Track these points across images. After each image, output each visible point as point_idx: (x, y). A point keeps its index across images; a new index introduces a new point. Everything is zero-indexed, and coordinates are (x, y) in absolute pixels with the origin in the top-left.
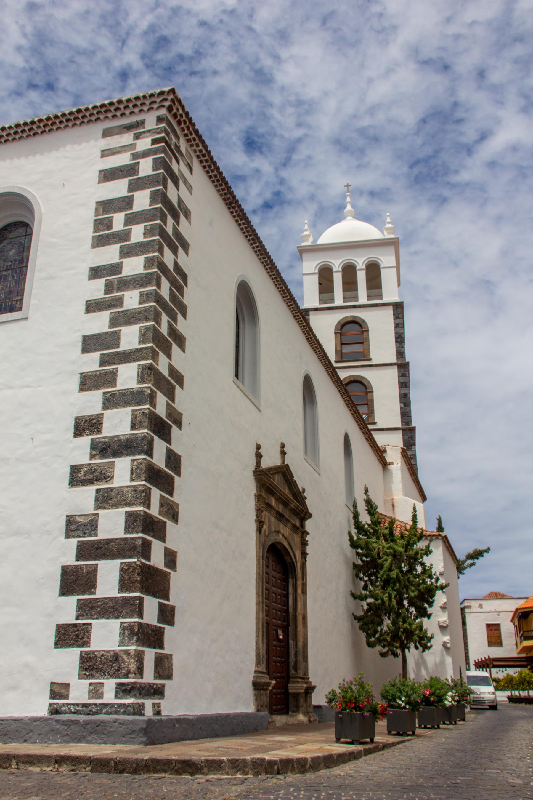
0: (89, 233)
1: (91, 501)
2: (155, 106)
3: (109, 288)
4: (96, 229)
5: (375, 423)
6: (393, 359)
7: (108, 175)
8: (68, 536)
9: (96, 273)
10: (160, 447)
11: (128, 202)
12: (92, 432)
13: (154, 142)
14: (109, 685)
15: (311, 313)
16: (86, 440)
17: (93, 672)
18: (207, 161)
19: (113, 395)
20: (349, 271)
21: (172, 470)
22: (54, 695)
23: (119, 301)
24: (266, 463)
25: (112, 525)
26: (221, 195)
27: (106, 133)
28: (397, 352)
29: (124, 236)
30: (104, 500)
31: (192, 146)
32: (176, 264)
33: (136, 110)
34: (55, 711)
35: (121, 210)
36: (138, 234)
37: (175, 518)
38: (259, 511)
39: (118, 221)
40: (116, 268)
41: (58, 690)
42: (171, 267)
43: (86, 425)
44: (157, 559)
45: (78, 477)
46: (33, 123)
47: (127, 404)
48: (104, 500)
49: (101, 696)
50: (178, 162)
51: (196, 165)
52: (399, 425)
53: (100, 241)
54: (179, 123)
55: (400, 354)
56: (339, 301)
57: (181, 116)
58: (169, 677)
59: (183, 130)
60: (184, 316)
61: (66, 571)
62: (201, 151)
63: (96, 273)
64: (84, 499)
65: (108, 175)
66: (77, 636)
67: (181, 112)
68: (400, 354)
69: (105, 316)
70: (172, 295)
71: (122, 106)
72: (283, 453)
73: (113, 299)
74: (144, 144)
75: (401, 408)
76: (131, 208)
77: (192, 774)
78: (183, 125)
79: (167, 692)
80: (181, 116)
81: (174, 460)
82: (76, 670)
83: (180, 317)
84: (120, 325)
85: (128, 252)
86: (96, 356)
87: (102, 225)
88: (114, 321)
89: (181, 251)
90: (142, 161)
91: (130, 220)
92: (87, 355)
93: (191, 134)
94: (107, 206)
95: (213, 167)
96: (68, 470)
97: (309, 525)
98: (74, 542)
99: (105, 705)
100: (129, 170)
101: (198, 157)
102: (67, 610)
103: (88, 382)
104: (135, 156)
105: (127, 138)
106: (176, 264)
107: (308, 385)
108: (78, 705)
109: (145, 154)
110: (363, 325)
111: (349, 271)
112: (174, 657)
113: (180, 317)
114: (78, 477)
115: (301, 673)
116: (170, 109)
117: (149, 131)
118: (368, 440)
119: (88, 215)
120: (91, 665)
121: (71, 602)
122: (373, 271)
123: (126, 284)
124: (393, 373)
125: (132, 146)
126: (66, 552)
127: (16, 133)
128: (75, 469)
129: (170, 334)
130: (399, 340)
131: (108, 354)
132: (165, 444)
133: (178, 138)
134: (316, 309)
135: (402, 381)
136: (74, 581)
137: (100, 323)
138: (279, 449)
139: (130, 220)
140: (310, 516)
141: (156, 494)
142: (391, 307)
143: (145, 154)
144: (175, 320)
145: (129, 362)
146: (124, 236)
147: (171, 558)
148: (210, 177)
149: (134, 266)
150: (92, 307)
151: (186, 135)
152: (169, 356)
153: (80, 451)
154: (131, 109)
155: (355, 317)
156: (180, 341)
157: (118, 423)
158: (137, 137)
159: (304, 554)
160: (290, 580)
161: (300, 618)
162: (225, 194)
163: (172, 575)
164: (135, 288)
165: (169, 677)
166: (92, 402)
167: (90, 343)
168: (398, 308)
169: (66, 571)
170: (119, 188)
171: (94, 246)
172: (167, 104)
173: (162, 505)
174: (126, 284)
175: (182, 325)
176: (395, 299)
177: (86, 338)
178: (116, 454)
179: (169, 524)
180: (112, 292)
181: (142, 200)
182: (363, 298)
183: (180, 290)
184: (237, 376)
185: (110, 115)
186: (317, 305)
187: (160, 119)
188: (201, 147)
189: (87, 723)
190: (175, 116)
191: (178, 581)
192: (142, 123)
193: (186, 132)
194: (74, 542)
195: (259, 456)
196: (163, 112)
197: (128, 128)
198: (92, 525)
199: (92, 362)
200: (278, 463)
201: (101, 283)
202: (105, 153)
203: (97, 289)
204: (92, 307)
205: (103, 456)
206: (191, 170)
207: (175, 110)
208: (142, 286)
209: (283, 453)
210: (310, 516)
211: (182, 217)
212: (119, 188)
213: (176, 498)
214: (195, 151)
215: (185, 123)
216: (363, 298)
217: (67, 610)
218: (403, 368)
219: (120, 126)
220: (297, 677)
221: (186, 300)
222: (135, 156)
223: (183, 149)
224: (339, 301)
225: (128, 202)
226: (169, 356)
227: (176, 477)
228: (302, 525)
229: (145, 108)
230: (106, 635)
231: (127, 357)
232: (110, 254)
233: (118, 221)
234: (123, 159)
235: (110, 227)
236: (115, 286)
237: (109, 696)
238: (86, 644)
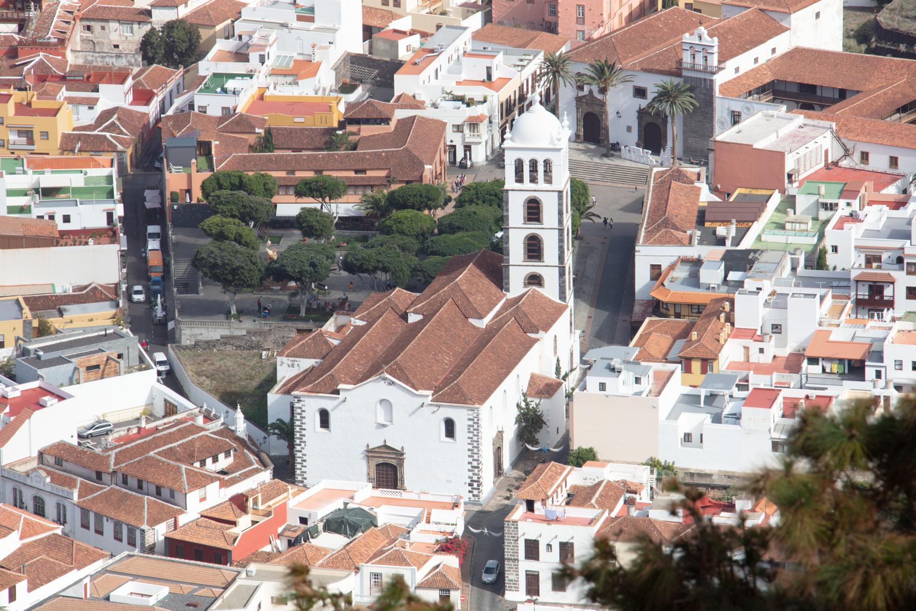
7: (469, 419)
39: (472, 429)
64: (471, 474)
65: (469, 419)
100: (472, 420)
105: (471, 413)
119: (466, 427)
120: (474, 496)
126: (469, 481)
137: (470, 447)
153: (469, 467)
166: (470, 460)
167: (469, 450)
170: (471, 423)
199: (470, 453)
203: (469, 441)
212: (471, 423)
232: (471, 435)
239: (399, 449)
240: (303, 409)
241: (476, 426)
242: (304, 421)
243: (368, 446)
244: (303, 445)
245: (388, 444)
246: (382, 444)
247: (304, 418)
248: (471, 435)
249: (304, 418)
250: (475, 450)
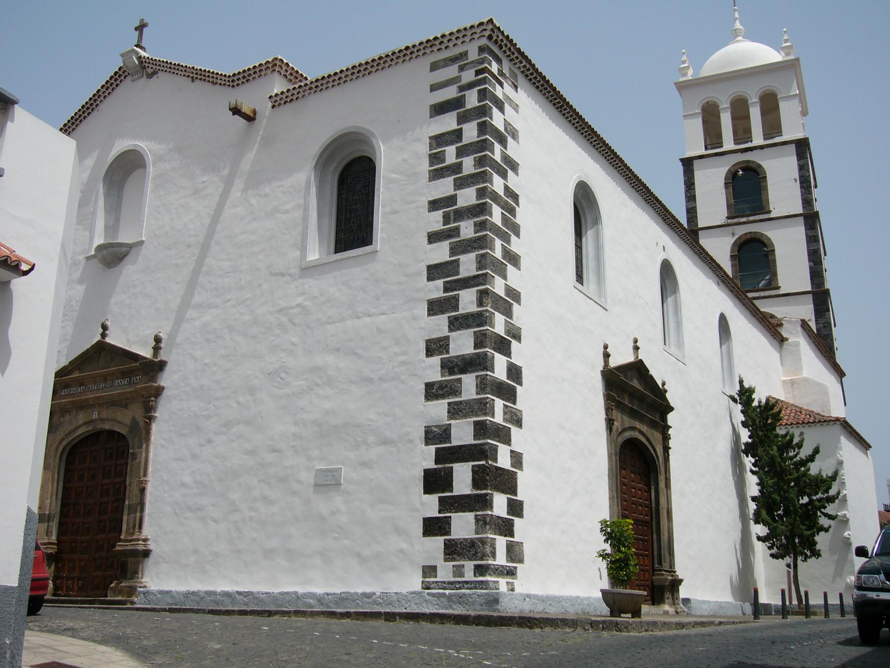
0: (425, 167)
1: (445, 413)
2: (476, 36)
3: (446, 219)
4: (431, 164)
5: (779, 288)
6: (797, 208)
8: (427, 444)
9: (434, 205)
10: (500, 364)
11: (457, 135)
12: (441, 353)
13: (478, 73)
14: (469, 566)
16: (436, 360)
17: (455, 556)
18: (532, 74)
19: (456, 318)
21: (513, 381)
22: (425, 575)
23: (456, 231)
24: (614, 363)
25: (463, 433)
26: (551, 101)
27: (434, 67)
28: (803, 200)
29: (456, 168)
30: (455, 411)
31: (515, 64)
32: (507, 188)
33: (459, 42)
34: (426, 586)
35: (452, 143)
36: (469, 165)
37: (518, 423)
38: (608, 410)
39: (450, 152)
40: (451, 200)
41: (429, 571)
42: (501, 192)
43: (435, 346)
44: (504, 461)
45: (432, 392)
46: (367, 63)
47: (469, 326)
48: (455, 411)
49: (462, 575)
50: (501, 85)
51: (521, 80)
53: (436, 175)
54: (501, 47)
55: (807, 202)
56: (729, 144)
57: (502, 41)
58: (521, 561)
59: (505, 52)
60: (518, 235)
61: (428, 473)
62: (524, 66)
63: (434, 205)
64: (439, 410)
65: (439, 109)
66: (440, 527)
67: (501, 37)
68: (807, 202)
69: (445, 245)
70: (505, 220)
71: (445, 40)
72: (636, 348)
73: (451, 230)
74: (469, 76)
75: (811, 268)
76: (461, 141)
77: (530, 628)
78: (504, 48)
79: (519, 573)
80: (502, 41)
81: (515, 372)
82: (441, 556)
83: (513, 238)
84: (459, 254)
86: (440, 283)
87: (435, 158)
88: (454, 251)
89: (510, 173)
90: (467, 93)
91: (461, 152)
92: (431, 283)
93: (513, 54)
94: (439, 140)
95: (539, 78)
96: (423, 387)
97: (671, 418)
98: (432, 448)
99: (467, 582)
100: (456, 104)
101: (523, 72)
102: (431, 505)
103: (435, 307)
104: (462, 89)
105: (451, 71)
106: (507, 188)
107: (667, 271)
108: (444, 582)
109: (470, 86)
110: (759, 170)
112: (524, 545)
113: (513, 238)
114: (432, 392)
115: (666, 566)
116: (490, 38)
117: (472, 62)
118: (754, 316)
119: (423, 149)
120: (453, 550)
121: (433, 500)
123: (460, 215)
125: (456, 80)
127: (353, 74)
128: (429, 386)
129: (504, 257)
130: (804, 185)
131: (450, 281)
132: (505, 358)
133: (499, 61)
134: (701, 157)
135: (811, 234)
136: (435, 481)
137: (441, 253)
138: (632, 344)
139: (461, 152)
140: (672, 409)
141: (499, 404)
142: (793, 146)
144: (508, 241)
145: (468, 288)
146: (456, 168)
147: (517, 459)
148: (537, 87)
150: (434, 237)
151: (508, 56)
152: (505, 277)
153: (432, 370)
154: (454, 42)
155: (748, 162)
156: (514, 259)
157: (463, 344)
158: (462, 69)
159: (666, 449)
160: (652, 475)
161: (663, 514)
162: (555, 99)
163: (518, 475)
164: (469, 218)
165: (521, 561)
166: (439, 325)
167: (434, 272)
168: (802, 147)
169: (428, 473)
170: (448, 122)
171: (430, 180)
172: (487, 33)
173: (505, 413)
174: (460, 215)
175: (516, 245)
176: (800, 135)
177: (430, 268)
178: (463, 371)
179: (514, 430)
180: (449, 224)
181: (470, 132)
182: (758, 139)
183: (512, 211)
184: (580, 278)
185: (435, 49)
186: (703, 152)
187: (481, 50)
188: (524, 63)
189: (450, 596)
190: (496, 42)
191: (523, 479)
193: (508, 53)
194: (432, 448)
195: (607, 356)
196: (484, 41)
197: (453, 60)
198: (445, 433)
199: (436, 289)
200: (631, 359)
201: (439, 215)
202: (434, 88)
204: (434, 237)
205: (451, 374)
206: (516, 87)
207: (495, 38)
208: (475, 216)
209: (636, 348)
210: (672, 409)
211: (510, 139)
213: (519, 406)
214: (519, 68)
215: (506, 46)
216: (758, 139)
217: (431, 505)
218: (811, 219)
219: (445, 59)
220: (661, 570)
221: (518, 220)
222: (462, 89)
223: (506, 71)
224: (729, 144)
225: (457, 135)
226: (505, 277)
227: (518, 387)
228: (664, 419)
229: (467, 39)
230: (463, 525)
231: (466, 283)
234: (450, 93)
235: (444, 161)
236: (452, 217)
237: (469, 576)
238: (448, 533)
239: (146, 352)
241: (470, 132)
245: (114, 339)
248: (445, 187)
250: (468, 264)
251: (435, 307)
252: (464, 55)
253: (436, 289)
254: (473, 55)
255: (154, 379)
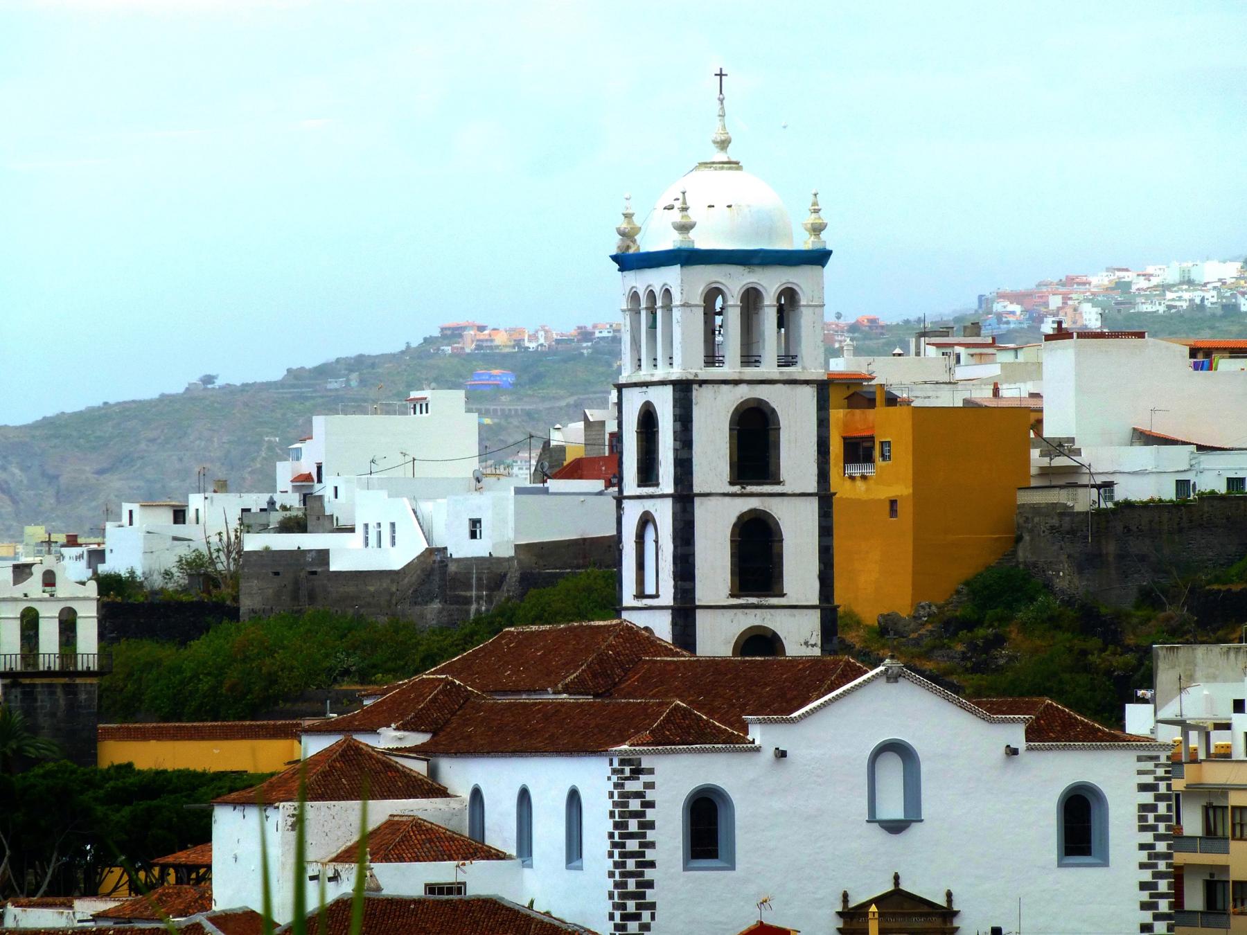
0: (1136, 823)
7: (1143, 788)
9: (1142, 847)
11: (1153, 808)
15: (695, 386)
20: (751, 298)
23: (1155, 866)
27: (1140, 759)
29: (1153, 828)
36: (1162, 828)
40: (1151, 847)
52: (817, 603)
53: (1143, 829)
63: (1142, 847)
65: (1143, 788)
74: (1161, 772)
85: (1158, 838)
87: (1142, 818)
94: (1144, 808)
103: (1144, 906)
104: (1156, 779)
105: (1150, 765)
109: (1162, 779)
111: (751, 298)
119: (1134, 812)
122: (789, 301)
124: (813, 506)
125: (1153, 772)
137: (1147, 876)
139: (1158, 819)
143: (1162, 779)
149: (1161, 847)
150: (1142, 866)
158: (1156, 766)
167: (1143, 886)
170: (1148, 798)
192: (1157, 758)
197: (1151, 758)
199: (1145, 896)
201: (1145, 853)
202: (1140, 773)
203: (1143, 856)
204: (1142, 866)
212: (1148, 798)
222: (1156, 779)
225: (1153, 808)
232: (1148, 837)
233: (1151, 816)
234: (1149, 779)
239: (941, 901)
240: (650, 795)
242: (651, 835)
243: (845, 896)
244: (646, 915)
245: (906, 886)
246: (889, 887)
247: (651, 825)
248: (1148, 837)
249: (651, 825)
251: (1144, 906)
252: (1157, 758)
253: (1145, 896)
254: (1163, 760)
255: (951, 922)
